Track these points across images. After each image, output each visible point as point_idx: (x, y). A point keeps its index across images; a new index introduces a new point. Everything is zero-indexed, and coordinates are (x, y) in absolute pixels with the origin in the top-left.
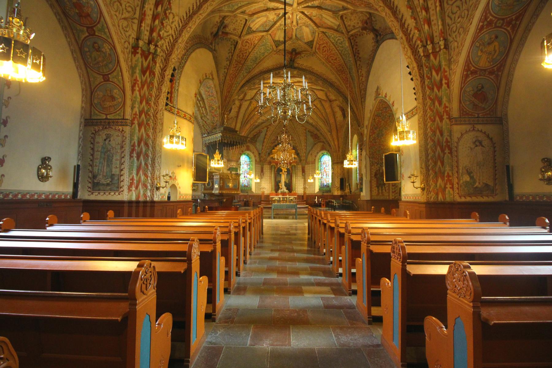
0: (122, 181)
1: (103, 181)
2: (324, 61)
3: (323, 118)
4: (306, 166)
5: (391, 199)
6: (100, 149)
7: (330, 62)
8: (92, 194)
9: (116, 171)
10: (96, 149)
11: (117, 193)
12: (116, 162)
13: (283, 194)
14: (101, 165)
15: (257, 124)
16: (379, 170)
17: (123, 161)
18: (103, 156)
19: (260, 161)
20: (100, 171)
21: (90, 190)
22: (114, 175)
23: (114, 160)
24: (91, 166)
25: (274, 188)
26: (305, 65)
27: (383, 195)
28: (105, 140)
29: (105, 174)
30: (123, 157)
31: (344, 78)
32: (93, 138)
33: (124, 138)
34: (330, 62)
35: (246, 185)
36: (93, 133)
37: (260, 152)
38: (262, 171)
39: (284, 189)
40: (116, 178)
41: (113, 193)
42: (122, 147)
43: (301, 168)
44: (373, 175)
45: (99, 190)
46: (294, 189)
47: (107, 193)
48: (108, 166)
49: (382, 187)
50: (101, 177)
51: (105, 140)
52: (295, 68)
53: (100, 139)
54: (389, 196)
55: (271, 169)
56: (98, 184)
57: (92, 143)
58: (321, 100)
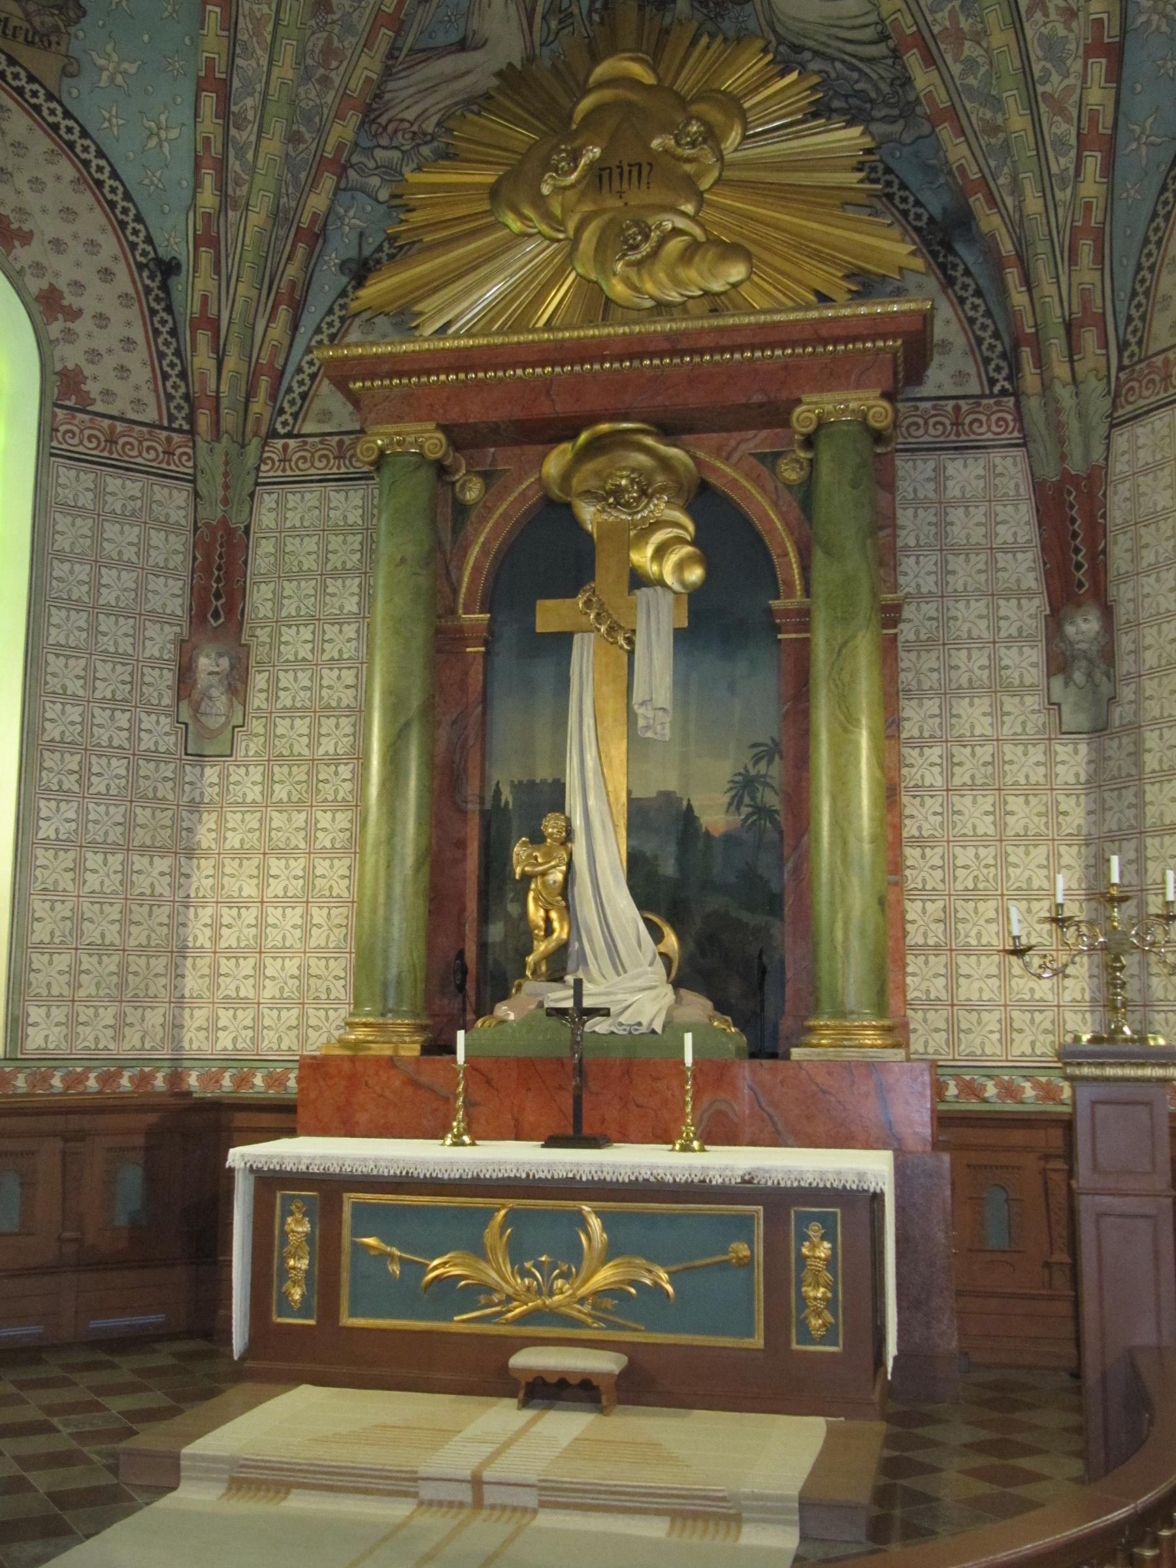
13: (585, 1087)
19: (186, 410)
25: (403, 949)
37: (174, 239)
38: (218, 591)
43: (1018, 523)
46: (847, 968)
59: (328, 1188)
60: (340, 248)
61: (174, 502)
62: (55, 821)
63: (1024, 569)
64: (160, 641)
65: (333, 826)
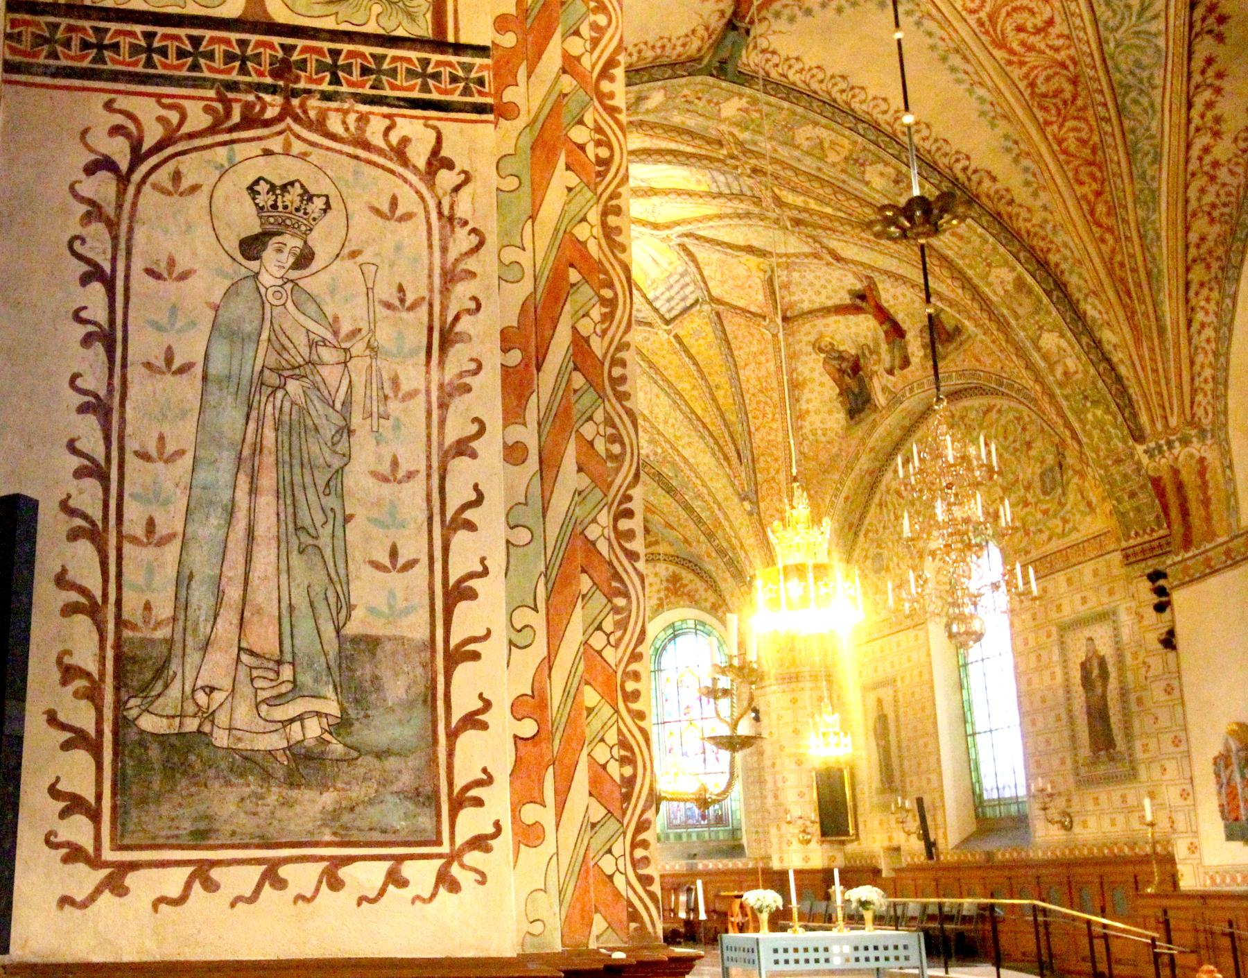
0: (473, 721)
1: (244, 724)
2: (964, 32)
6: (190, 349)
7: (1002, 45)
8: (115, 883)
9: (388, 604)
10: (143, 344)
11: (421, 873)
12: (382, 507)
14: (209, 527)
17: (458, 494)
18: (230, 417)
20: (201, 596)
21: (78, 830)
22: (371, 644)
23: (358, 479)
24: (95, 535)
26: (809, 62)
28: (252, 247)
29: (264, 637)
30: (463, 448)
31: (1072, 145)
32: (115, 222)
33: (462, 241)
34: (1002, 45)
36: (105, 164)
40: (398, 686)
41: (302, 876)
42: (444, 338)
45: (201, 837)
47: (302, 876)
48: (298, 535)
50: (217, 667)
51: (252, 247)
52: (745, 79)
53: (191, 226)
56: (184, 755)
57: (94, 274)
58: (720, 311)
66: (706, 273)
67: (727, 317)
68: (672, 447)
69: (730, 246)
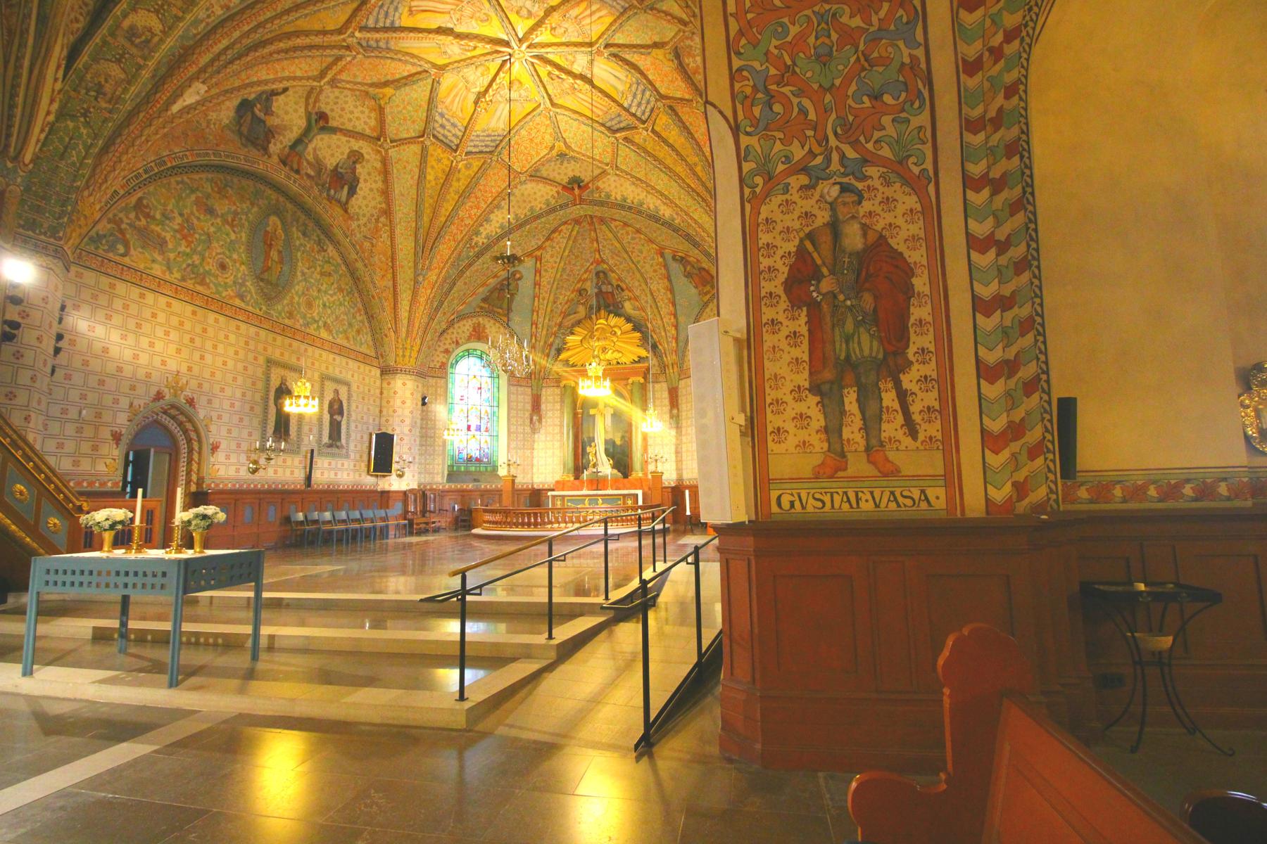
3: (700, 189)
4: (682, 383)
5: (974, 505)
13: (598, 482)
15: (481, 240)
16: (834, 227)
25: (571, 464)
27: (891, 472)
35: (475, 454)
39: (606, 468)
43: (666, 395)
44: (774, 285)
49: (867, 395)
54: (952, 478)
55: (562, 401)
58: (672, 106)
59: (563, 496)
60: (555, 346)
61: (529, 390)
62: (513, 445)
63: (667, 402)
64: (527, 414)
65: (557, 444)
66: (650, 77)
67: (679, 109)
68: (687, 214)
69: (642, 46)
